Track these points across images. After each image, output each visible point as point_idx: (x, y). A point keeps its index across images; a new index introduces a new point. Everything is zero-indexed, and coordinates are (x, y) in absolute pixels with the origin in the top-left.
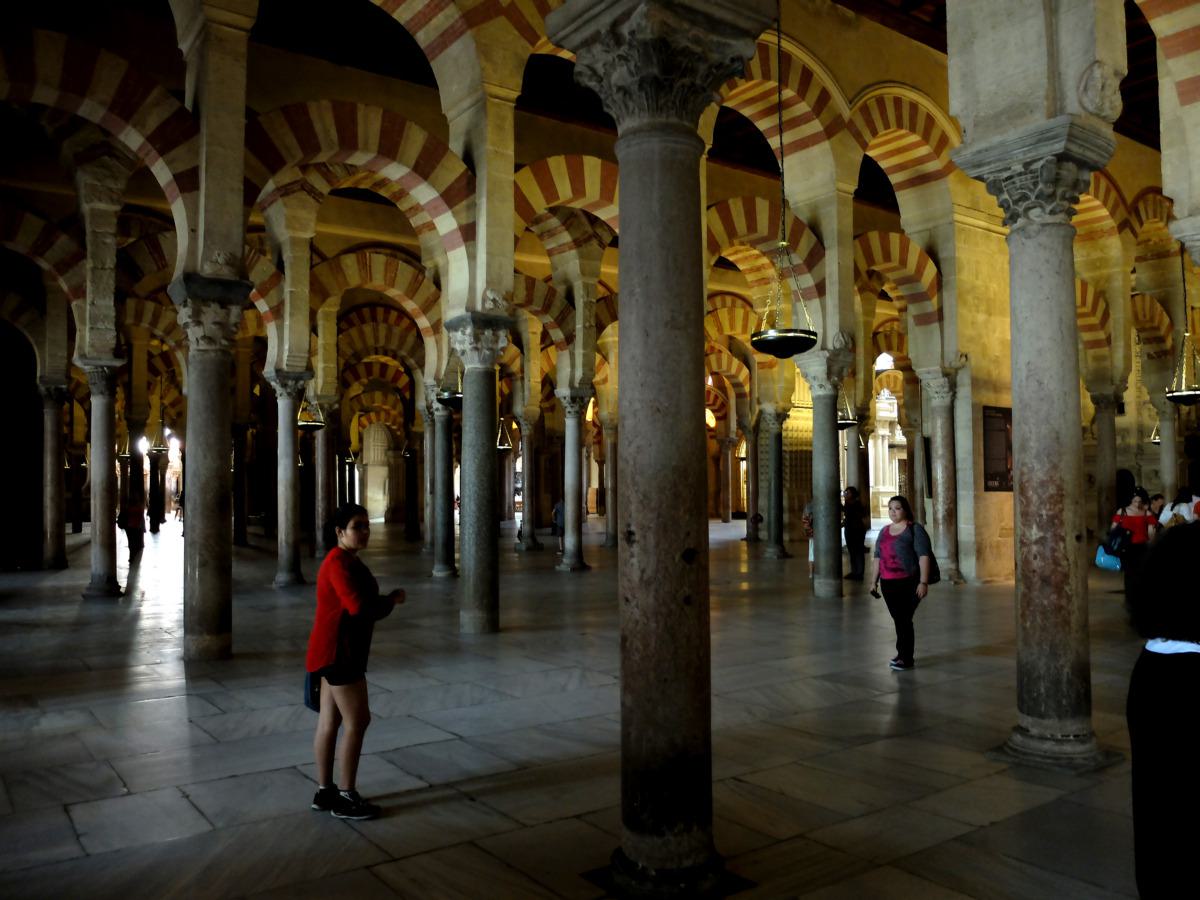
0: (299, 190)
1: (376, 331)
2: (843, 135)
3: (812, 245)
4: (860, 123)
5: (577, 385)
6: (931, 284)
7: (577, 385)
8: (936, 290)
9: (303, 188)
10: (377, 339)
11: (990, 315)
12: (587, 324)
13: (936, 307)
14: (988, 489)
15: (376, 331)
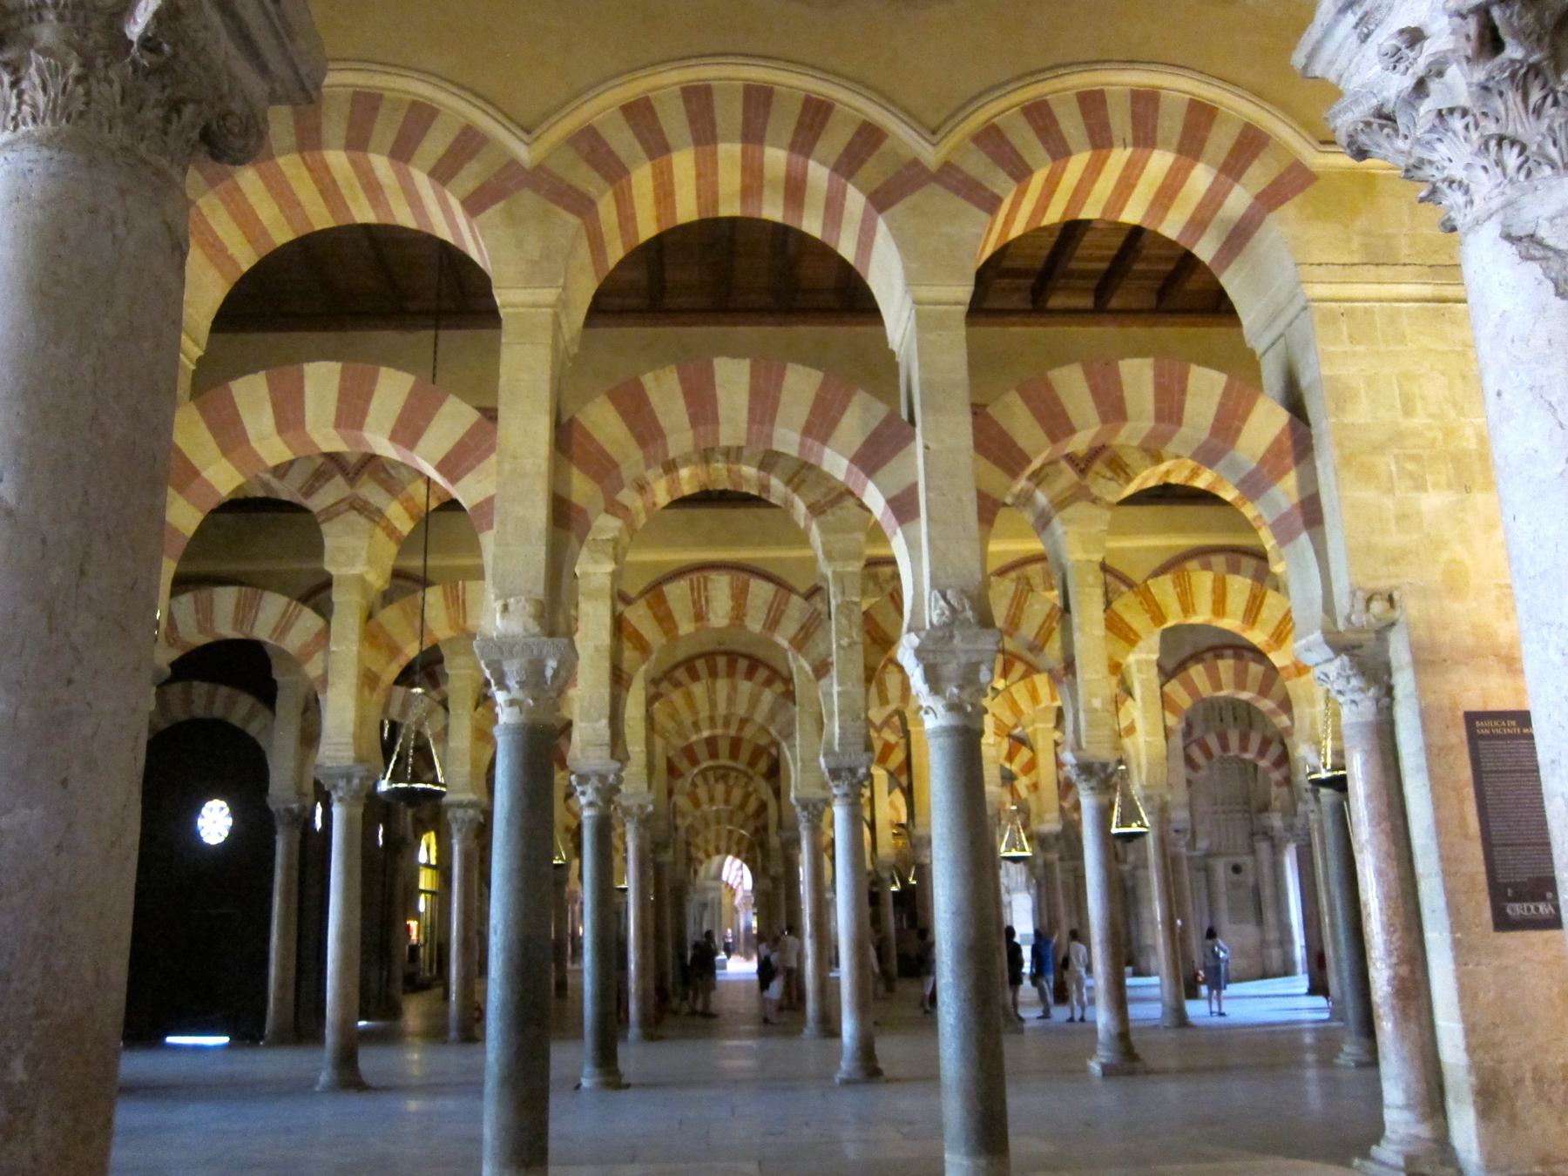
0: (347, 510)
1: (711, 692)
2: (934, 197)
3: (875, 424)
4: (977, 165)
5: (837, 748)
6: (1275, 449)
7: (837, 748)
8: (1289, 460)
9: (353, 507)
10: (713, 705)
11: (1468, 490)
12: (845, 642)
13: (1295, 498)
14: (1503, 923)
15: (711, 692)
